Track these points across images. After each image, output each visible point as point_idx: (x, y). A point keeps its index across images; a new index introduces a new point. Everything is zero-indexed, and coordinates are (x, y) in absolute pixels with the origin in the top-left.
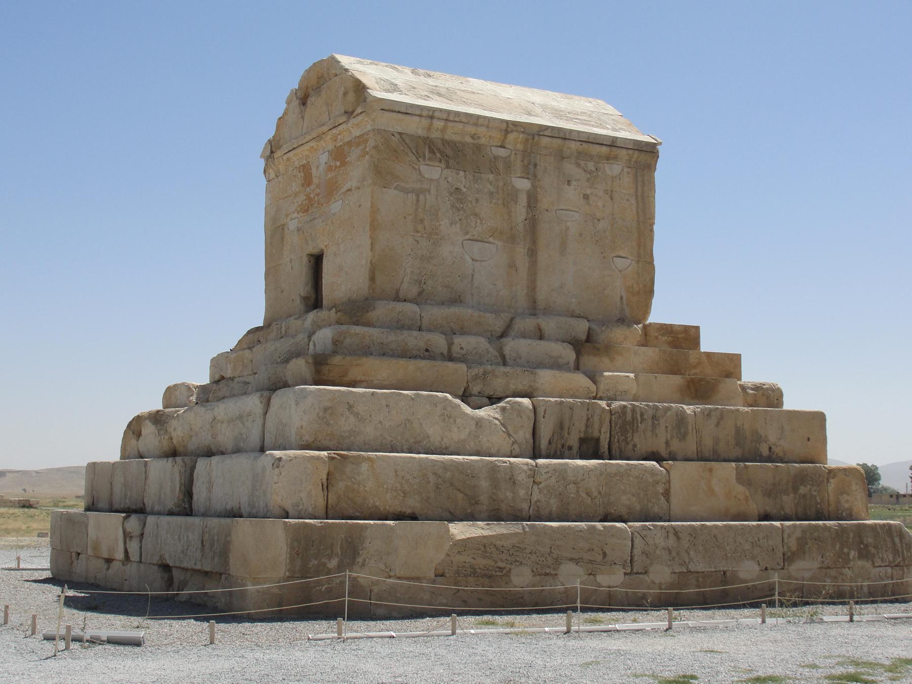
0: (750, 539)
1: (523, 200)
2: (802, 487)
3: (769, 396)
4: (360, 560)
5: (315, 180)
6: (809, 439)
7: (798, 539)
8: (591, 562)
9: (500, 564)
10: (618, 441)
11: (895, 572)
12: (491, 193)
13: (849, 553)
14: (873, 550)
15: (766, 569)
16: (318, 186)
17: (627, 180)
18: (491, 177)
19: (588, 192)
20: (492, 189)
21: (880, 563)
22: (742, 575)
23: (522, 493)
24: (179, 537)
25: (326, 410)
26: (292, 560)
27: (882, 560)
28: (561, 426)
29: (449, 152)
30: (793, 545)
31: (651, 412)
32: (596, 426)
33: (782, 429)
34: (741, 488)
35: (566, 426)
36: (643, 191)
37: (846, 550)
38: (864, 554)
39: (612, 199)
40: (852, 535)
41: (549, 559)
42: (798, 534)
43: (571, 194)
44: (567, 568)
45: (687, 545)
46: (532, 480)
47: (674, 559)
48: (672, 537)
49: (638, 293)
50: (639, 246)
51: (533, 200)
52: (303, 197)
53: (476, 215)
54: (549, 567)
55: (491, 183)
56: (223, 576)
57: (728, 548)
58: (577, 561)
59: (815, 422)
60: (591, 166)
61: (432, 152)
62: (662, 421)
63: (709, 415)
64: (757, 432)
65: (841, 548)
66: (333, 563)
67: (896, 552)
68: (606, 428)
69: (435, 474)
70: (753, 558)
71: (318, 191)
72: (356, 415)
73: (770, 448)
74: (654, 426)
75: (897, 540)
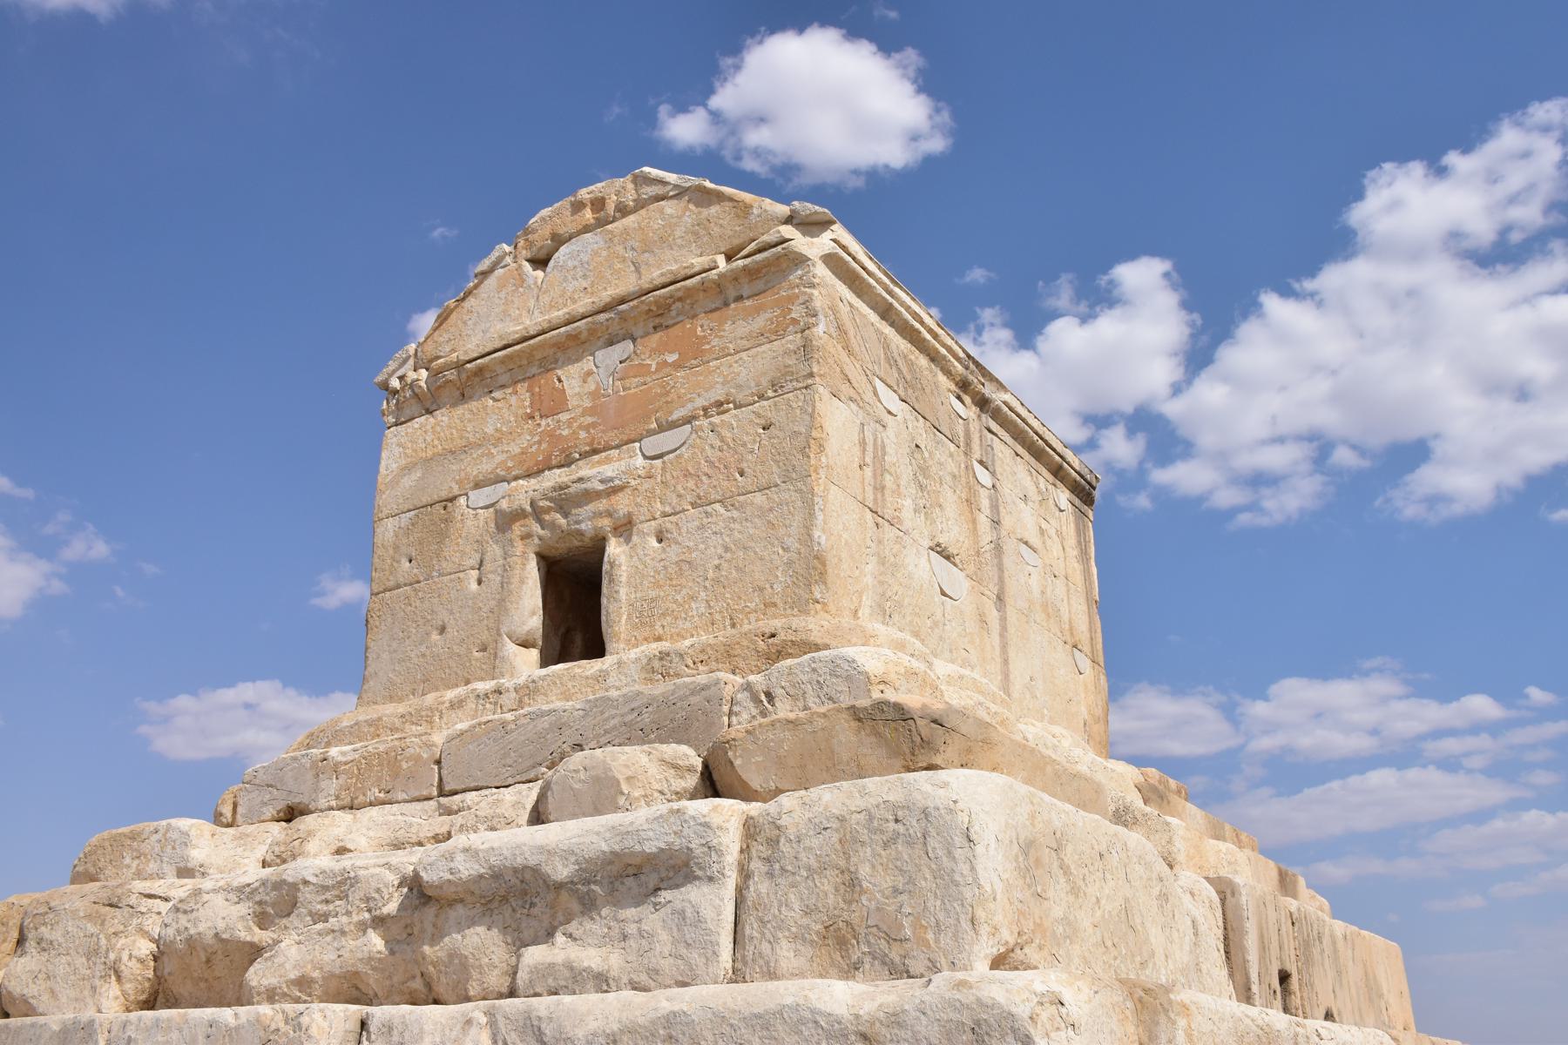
1: (985, 503)
12: (954, 476)
19: (1044, 525)
25: (1027, 847)
29: (909, 378)
52: (525, 441)
55: (951, 455)
61: (887, 359)
71: (589, 420)
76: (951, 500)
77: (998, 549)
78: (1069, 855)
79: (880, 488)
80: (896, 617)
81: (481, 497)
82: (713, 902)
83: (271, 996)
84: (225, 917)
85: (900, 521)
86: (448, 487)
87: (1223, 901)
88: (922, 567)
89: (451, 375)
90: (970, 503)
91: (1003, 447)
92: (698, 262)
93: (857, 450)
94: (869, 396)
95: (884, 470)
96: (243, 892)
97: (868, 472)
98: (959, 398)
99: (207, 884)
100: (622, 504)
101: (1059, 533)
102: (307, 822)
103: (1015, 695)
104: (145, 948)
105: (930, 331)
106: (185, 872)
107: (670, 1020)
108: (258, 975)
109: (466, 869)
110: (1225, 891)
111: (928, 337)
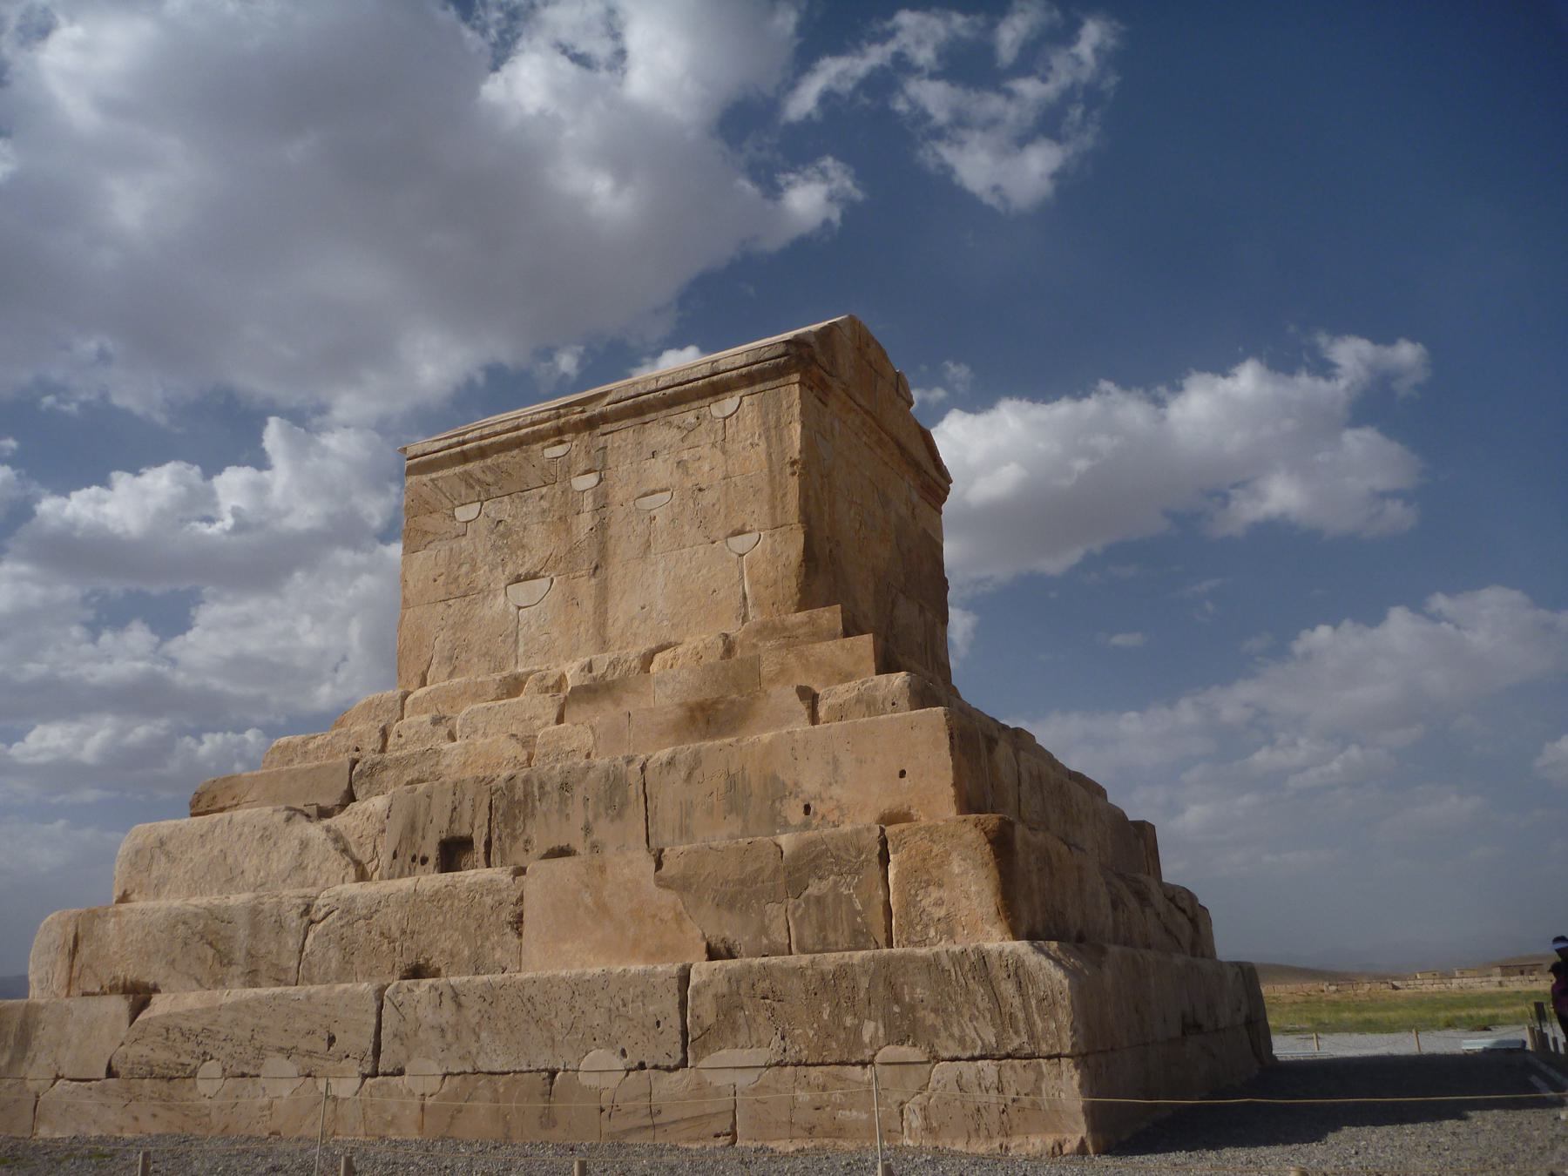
0: (606, 1003)
1: (588, 504)
2: (813, 882)
4: (30, 1054)
6: (902, 774)
7: (716, 996)
8: (310, 1053)
9: (185, 1059)
10: (500, 838)
11: (1008, 1074)
13: (857, 1031)
14: (931, 1019)
15: (642, 1066)
17: (750, 415)
19: (685, 455)
20: (545, 504)
21: (959, 1053)
27: (962, 1041)
28: (412, 827)
29: (490, 478)
30: (704, 1009)
31: (558, 780)
32: (467, 817)
33: (835, 760)
34: (669, 897)
35: (420, 825)
36: (778, 420)
37: (849, 1021)
38: (904, 1029)
39: (724, 452)
40: (864, 982)
41: (250, 1049)
43: (660, 471)
44: (276, 1064)
45: (475, 1021)
46: (306, 919)
47: (449, 1046)
48: (448, 1003)
49: (776, 582)
50: (773, 508)
51: (602, 502)
53: (523, 546)
54: (247, 1063)
57: (557, 1025)
58: (288, 1053)
60: (690, 418)
62: (579, 792)
63: (671, 762)
64: (775, 778)
65: (836, 1016)
67: (1004, 1019)
69: (184, 923)
70: (610, 1043)
72: (168, 854)
73: (807, 809)
74: (563, 801)
75: (1008, 988)
77: (601, 527)
80: (463, 656)
85: (473, 588)
91: (623, 434)
98: (561, 442)
103: (612, 632)
105: (508, 431)
111: (504, 437)
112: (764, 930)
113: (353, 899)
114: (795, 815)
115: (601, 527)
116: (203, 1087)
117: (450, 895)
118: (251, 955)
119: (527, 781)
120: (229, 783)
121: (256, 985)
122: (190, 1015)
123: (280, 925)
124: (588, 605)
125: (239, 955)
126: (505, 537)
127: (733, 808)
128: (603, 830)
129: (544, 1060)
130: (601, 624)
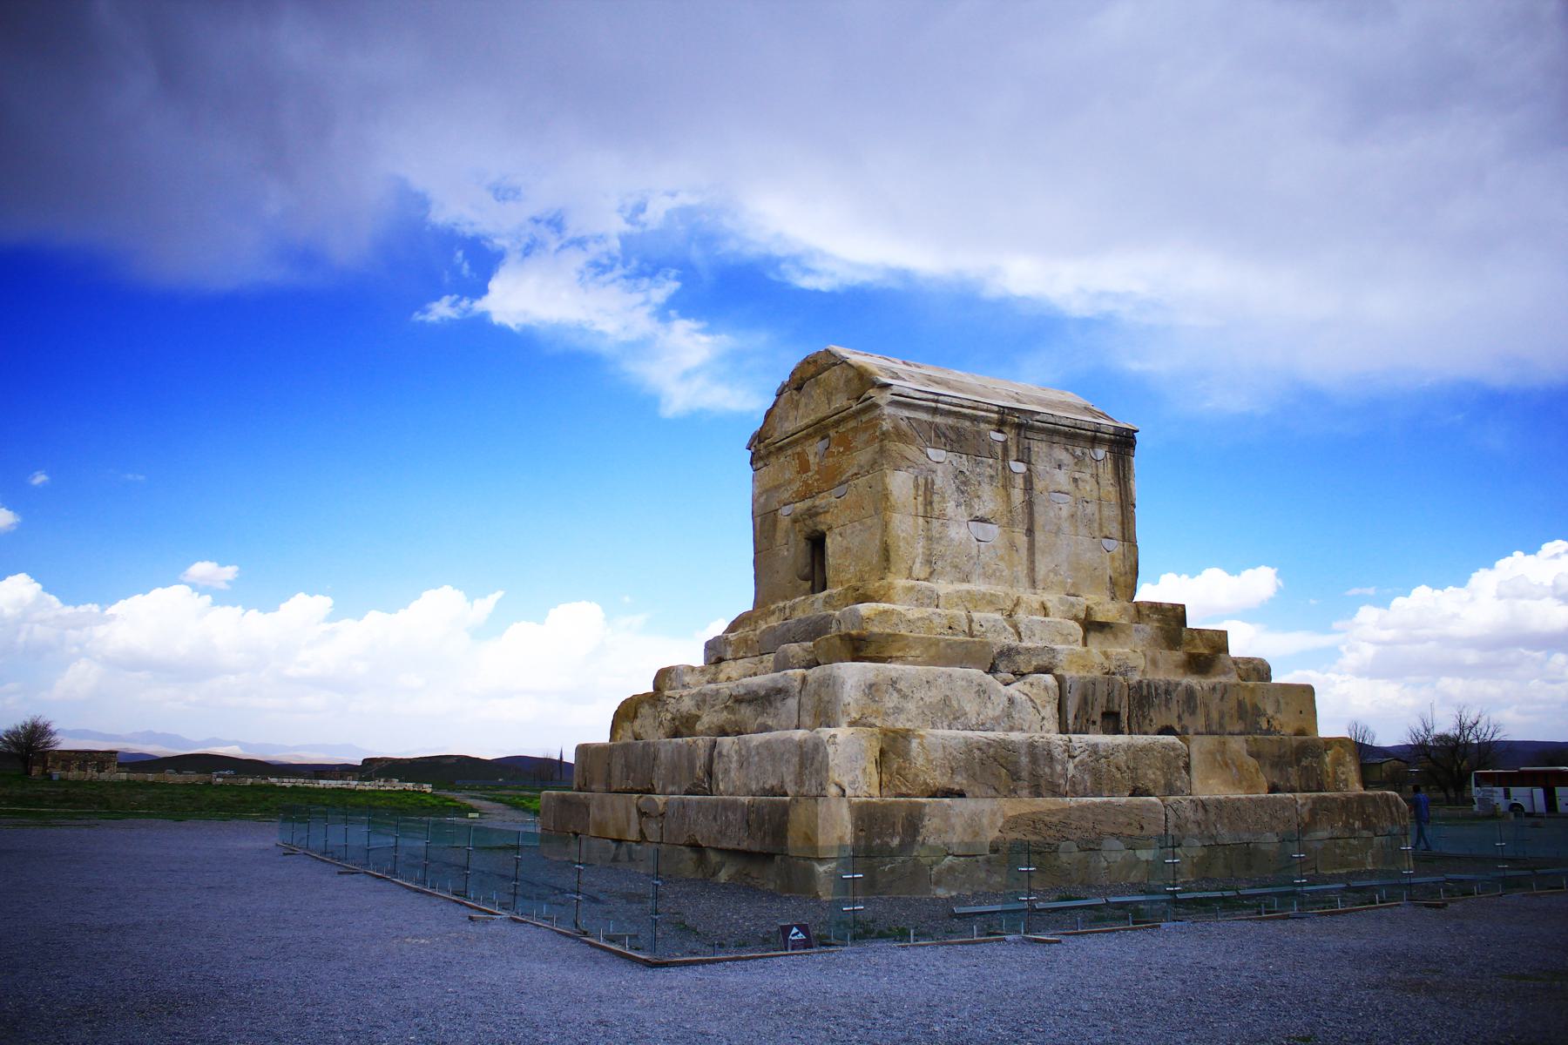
1: (1019, 482)
3: (1258, 670)
4: (920, 839)
5: (814, 468)
8: (1130, 836)
16: (817, 472)
18: (991, 461)
19: (1077, 475)
22: (1264, 847)
23: (1059, 768)
24: (715, 818)
25: (871, 686)
26: (857, 838)
34: (1252, 761)
42: (1310, 805)
52: (798, 484)
56: (778, 858)
58: (1118, 836)
59: (1306, 693)
60: (1078, 452)
63: (1214, 688)
66: (896, 842)
68: (1125, 702)
70: (1272, 829)
72: (899, 691)
74: (1167, 701)
76: (987, 491)
77: (1030, 504)
78: (901, 685)
79: (929, 503)
81: (786, 510)
82: (792, 703)
83: (702, 733)
84: (687, 705)
86: (775, 505)
87: (1060, 687)
88: (959, 532)
89: (772, 448)
90: (1007, 484)
92: (845, 403)
93: (913, 491)
94: (923, 458)
95: (933, 493)
96: (692, 696)
97: (920, 499)
98: (999, 431)
99: (685, 693)
100: (829, 518)
101: (1096, 477)
102: (723, 664)
104: (669, 716)
106: (684, 686)
107: (768, 742)
108: (699, 727)
109: (742, 691)
110: (1060, 680)
112: (1288, 780)
113: (1096, 745)
114: (1265, 726)
115: (1030, 504)
116: (1064, 858)
117: (1152, 749)
118: (1034, 775)
119: (1148, 685)
120: (893, 638)
121: (1039, 795)
122: (1051, 813)
123: (1050, 757)
124: (1024, 553)
125: (1024, 774)
126: (963, 482)
127: (1240, 718)
128: (1187, 719)
129: (1246, 837)
130: (1032, 569)
